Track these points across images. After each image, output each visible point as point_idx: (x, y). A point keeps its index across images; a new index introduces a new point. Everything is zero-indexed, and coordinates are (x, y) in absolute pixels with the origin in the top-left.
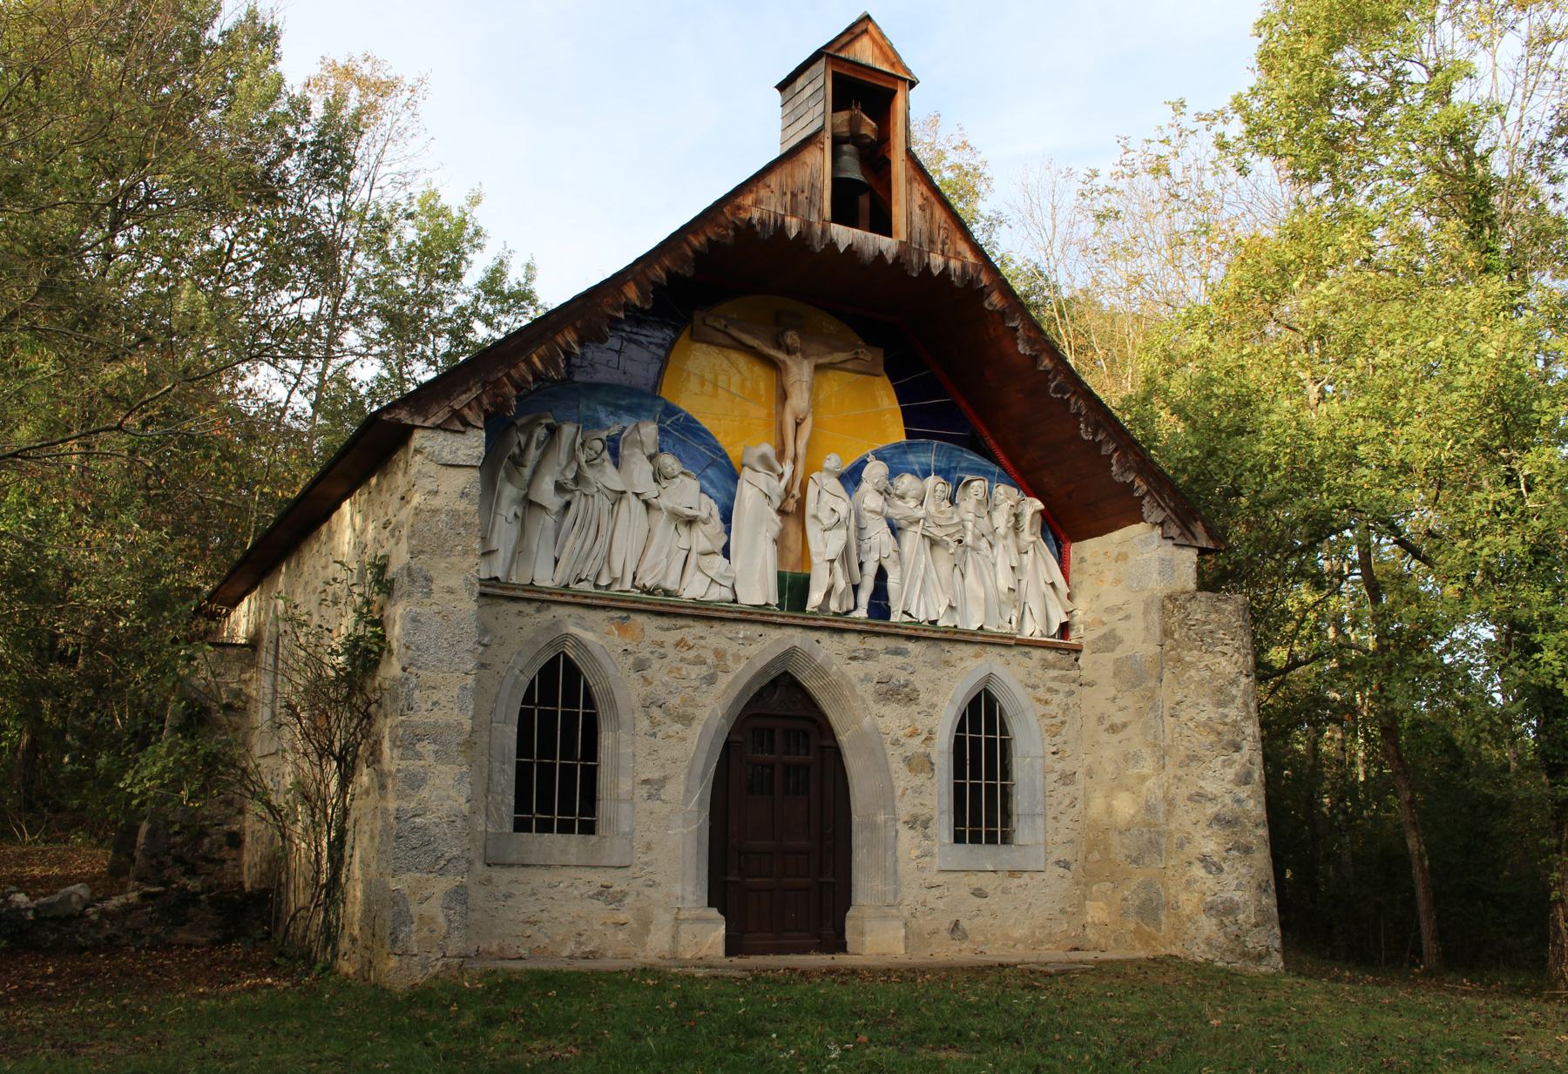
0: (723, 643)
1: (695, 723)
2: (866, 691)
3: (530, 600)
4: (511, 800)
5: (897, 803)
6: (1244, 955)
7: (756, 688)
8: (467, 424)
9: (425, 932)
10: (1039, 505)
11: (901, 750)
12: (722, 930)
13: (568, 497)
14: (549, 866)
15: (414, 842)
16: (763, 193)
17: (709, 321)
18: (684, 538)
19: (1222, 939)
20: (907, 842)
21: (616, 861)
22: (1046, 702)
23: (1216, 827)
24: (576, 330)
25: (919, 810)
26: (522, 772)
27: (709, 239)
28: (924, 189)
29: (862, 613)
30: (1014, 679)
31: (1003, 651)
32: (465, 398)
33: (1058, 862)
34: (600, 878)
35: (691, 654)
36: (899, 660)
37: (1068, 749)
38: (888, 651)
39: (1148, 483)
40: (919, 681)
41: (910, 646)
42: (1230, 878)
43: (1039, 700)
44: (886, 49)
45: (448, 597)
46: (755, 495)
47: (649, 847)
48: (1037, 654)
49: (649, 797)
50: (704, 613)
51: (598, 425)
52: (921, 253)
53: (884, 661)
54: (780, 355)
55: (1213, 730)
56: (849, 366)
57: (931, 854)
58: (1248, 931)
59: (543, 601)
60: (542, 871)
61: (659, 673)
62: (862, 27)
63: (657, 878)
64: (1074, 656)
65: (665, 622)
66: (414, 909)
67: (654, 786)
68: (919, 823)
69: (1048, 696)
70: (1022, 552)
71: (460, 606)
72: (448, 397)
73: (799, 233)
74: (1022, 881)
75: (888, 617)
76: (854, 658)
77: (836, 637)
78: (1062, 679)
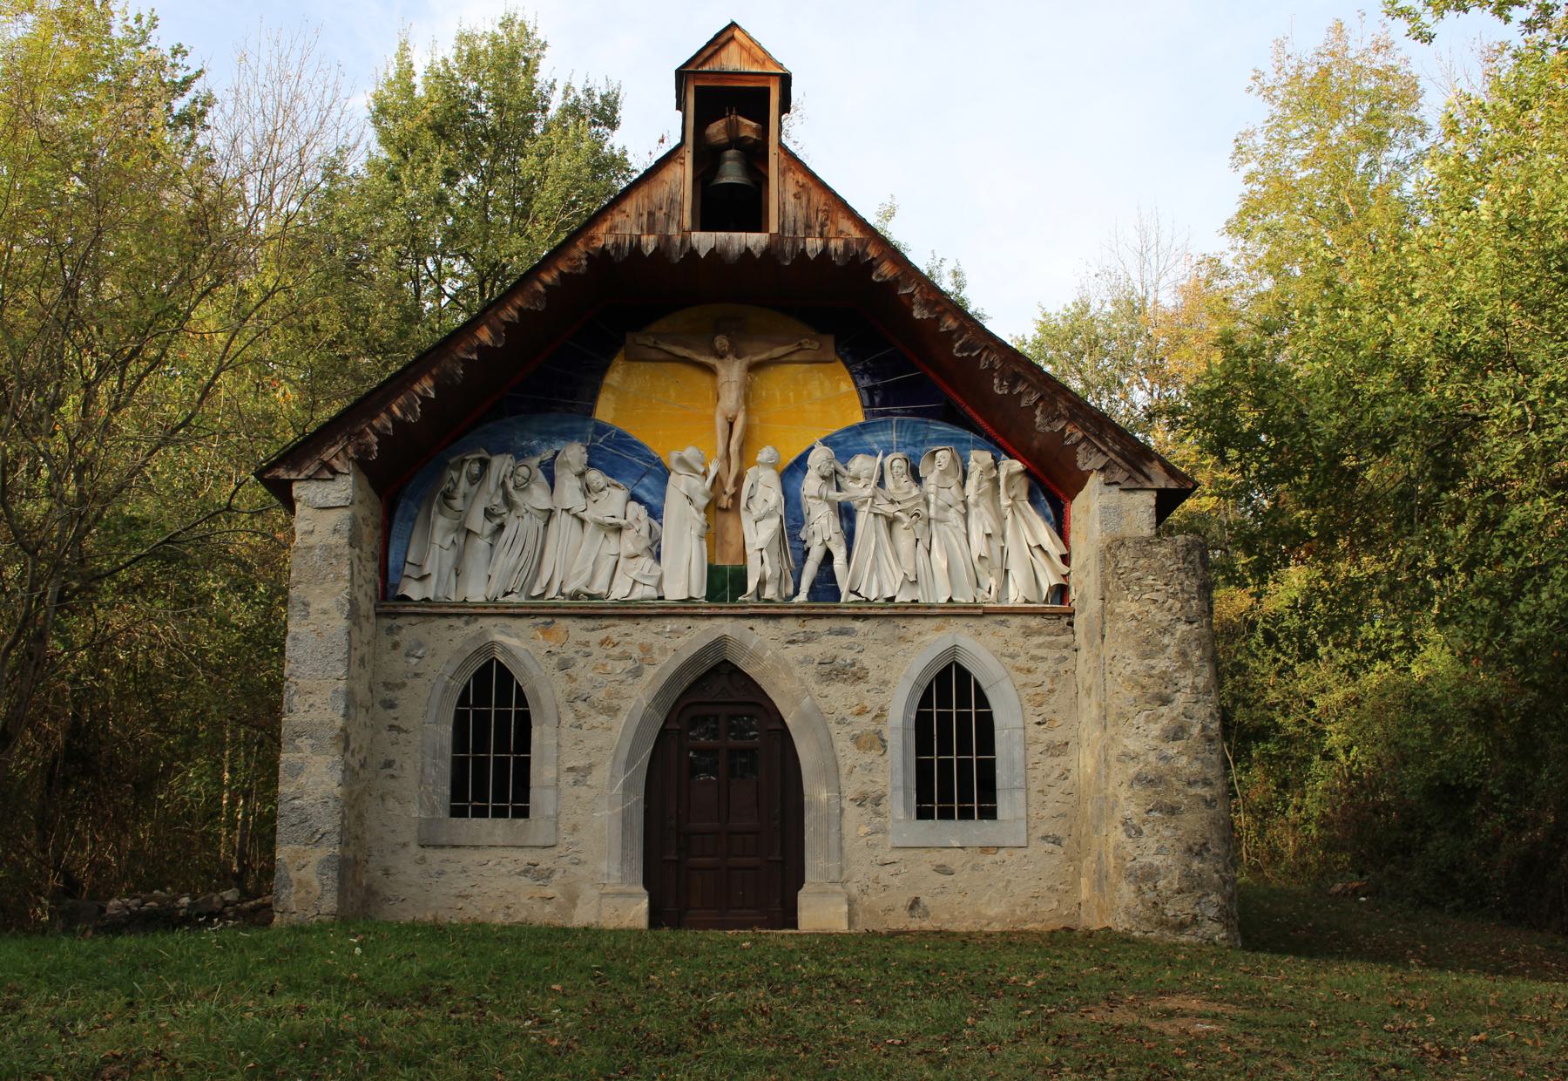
0: (648, 638)
1: (620, 714)
2: (809, 674)
3: (459, 615)
4: (446, 790)
5: (843, 781)
6: (1162, 923)
7: (691, 678)
8: (335, 472)
9: (302, 894)
10: (1017, 466)
11: (848, 729)
12: (645, 903)
13: (498, 521)
14: (477, 847)
15: (294, 820)
16: (618, 218)
17: (640, 340)
18: (612, 545)
19: (1139, 908)
20: (856, 822)
21: (540, 841)
22: (1029, 671)
23: (1137, 787)
24: (432, 377)
25: (869, 788)
26: (459, 767)
27: (561, 273)
28: (801, 178)
29: (802, 597)
30: (982, 650)
31: (972, 622)
32: (332, 451)
33: (1045, 838)
34: (526, 857)
35: (617, 651)
36: (845, 640)
37: (1059, 719)
38: (830, 632)
39: (1084, 429)
40: (866, 660)
41: (858, 625)
42: (1150, 843)
43: (1020, 670)
44: (754, 50)
45: (323, 617)
46: (684, 497)
47: (575, 828)
48: (1016, 622)
49: (575, 783)
50: (629, 612)
51: (533, 452)
52: (795, 242)
53: (826, 641)
54: (711, 361)
55: (1137, 683)
56: (795, 357)
57: (884, 831)
58: (1168, 899)
59: (471, 615)
60: (471, 851)
61: (584, 671)
62: (725, 37)
63: (582, 857)
64: (1066, 620)
65: (591, 623)
66: (293, 875)
67: (581, 774)
68: (871, 801)
69: (1032, 664)
70: (1001, 519)
71: (333, 623)
72: (319, 452)
73: (657, 249)
74: (997, 858)
75: (838, 599)
76: (793, 642)
77: (771, 623)
78: (1050, 645)
